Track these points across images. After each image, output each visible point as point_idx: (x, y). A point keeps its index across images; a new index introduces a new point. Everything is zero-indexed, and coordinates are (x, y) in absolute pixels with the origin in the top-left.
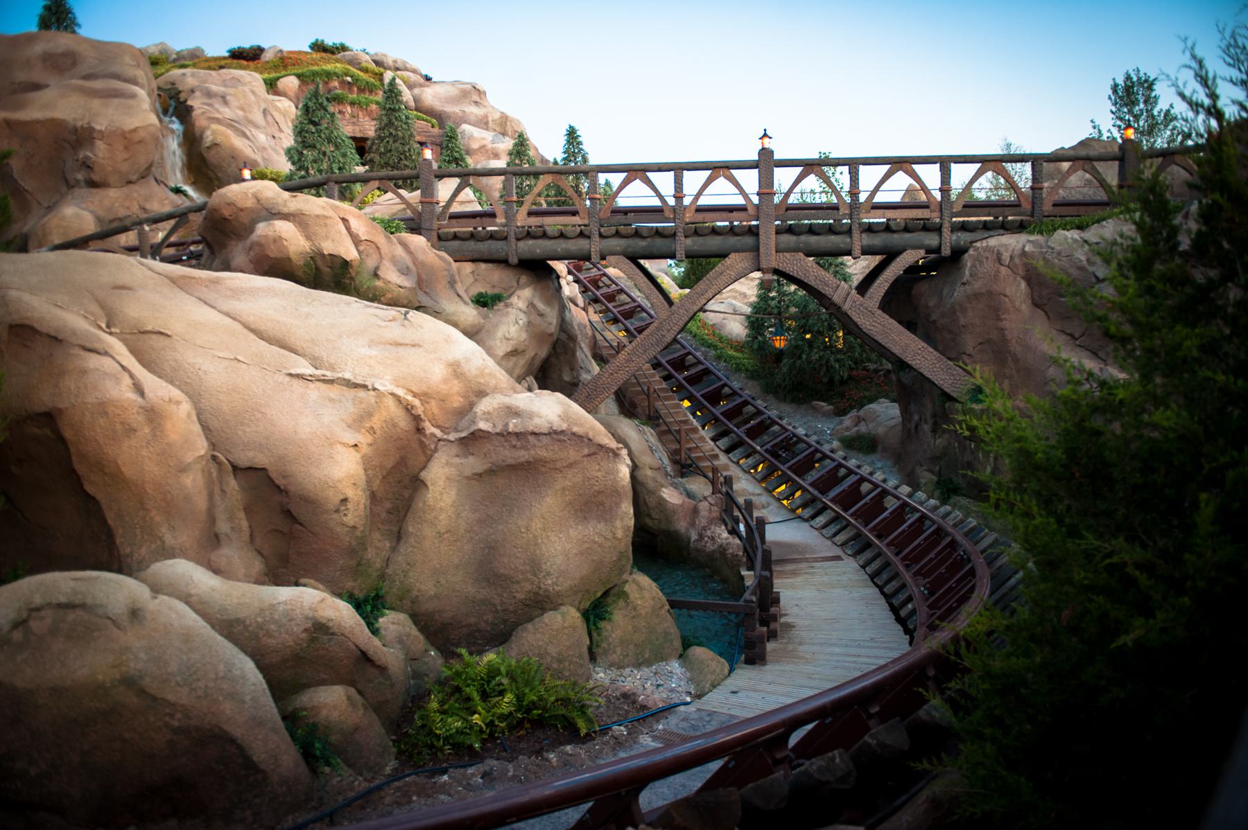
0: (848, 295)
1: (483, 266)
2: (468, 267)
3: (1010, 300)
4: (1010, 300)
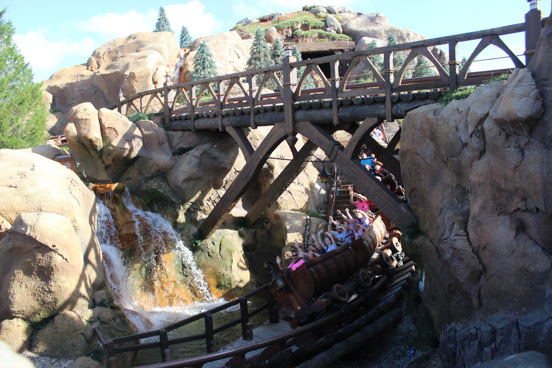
0: (333, 150)
1: (187, 133)
2: (180, 133)
3: (421, 157)
4: (421, 157)
